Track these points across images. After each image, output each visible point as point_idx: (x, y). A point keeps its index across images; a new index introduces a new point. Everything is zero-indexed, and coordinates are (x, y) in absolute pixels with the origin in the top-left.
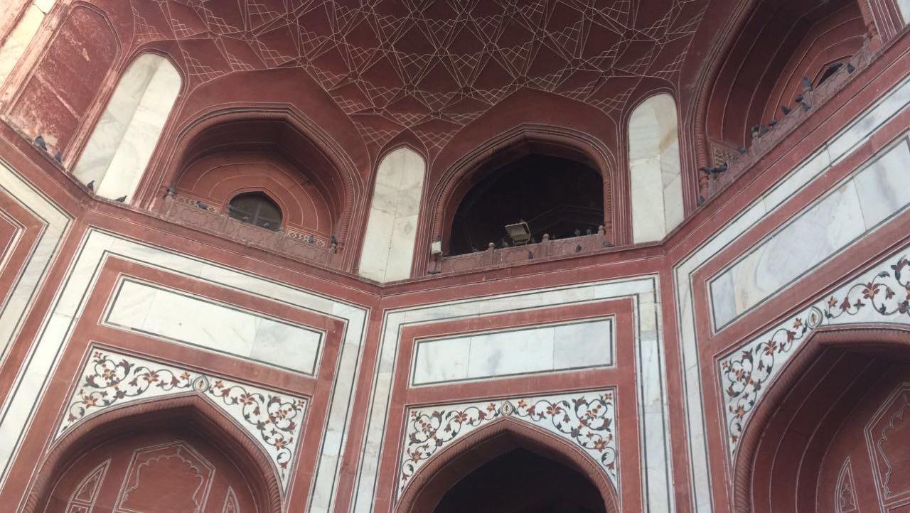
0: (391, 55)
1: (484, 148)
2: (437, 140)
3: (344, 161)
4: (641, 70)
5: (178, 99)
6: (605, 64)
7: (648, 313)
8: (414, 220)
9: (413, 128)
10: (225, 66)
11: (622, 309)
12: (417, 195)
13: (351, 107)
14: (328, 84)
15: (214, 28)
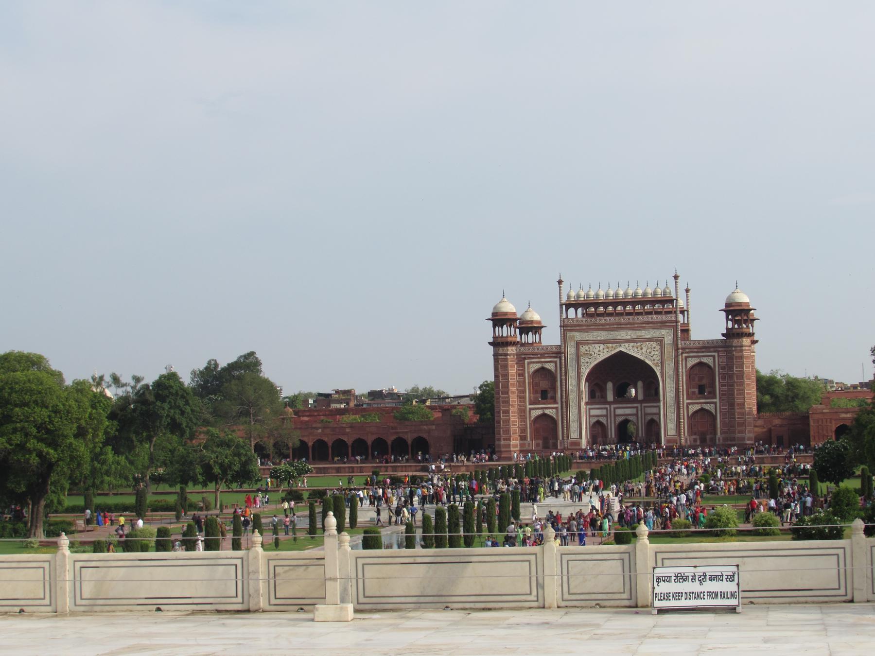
11: (637, 407)
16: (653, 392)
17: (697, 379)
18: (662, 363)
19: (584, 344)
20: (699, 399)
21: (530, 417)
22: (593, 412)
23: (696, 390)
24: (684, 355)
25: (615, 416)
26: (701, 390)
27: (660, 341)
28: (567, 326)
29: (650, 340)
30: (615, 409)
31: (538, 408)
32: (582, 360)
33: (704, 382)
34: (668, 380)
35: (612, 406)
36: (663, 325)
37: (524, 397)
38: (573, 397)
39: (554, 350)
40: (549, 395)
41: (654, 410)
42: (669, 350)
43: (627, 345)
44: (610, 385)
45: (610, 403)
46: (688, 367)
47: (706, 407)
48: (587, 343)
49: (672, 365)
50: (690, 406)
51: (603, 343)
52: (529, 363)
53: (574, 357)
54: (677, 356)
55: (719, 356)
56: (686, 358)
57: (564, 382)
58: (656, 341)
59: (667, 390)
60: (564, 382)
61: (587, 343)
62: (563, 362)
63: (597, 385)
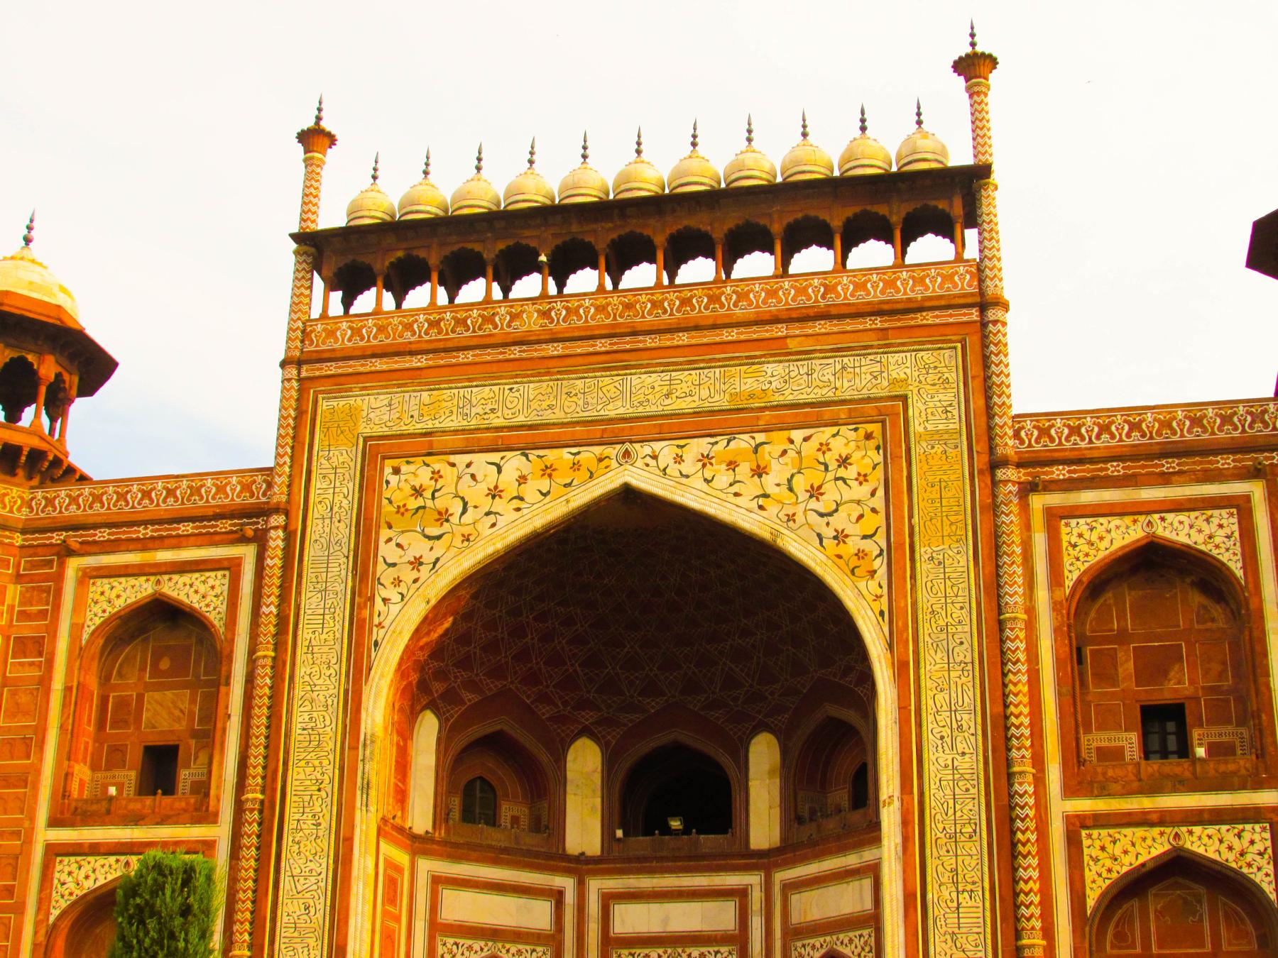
0: (575, 671)
1: (644, 747)
2: (609, 733)
3: (544, 757)
4: (759, 712)
5: (439, 739)
6: (735, 699)
7: (757, 896)
8: (599, 801)
9: (592, 724)
10: (462, 702)
11: (741, 894)
12: (597, 779)
13: (545, 711)
14: (528, 697)
15: (456, 677)
16: (841, 796)
17: (1127, 667)
18: (889, 552)
19: (408, 457)
20: (1153, 789)
21: (44, 902)
22: (462, 906)
23: (1130, 741)
24: (1038, 502)
25: (609, 942)
26: (1164, 726)
27: (885, 417)
28: (320, 358)
29: (812, 414)
30: (608, 900)
31: (95, 849)
32: (387, 551)
33: (1179, 684)
34: (932, 665)
35: (595, 886)
36: (894, 320)
37: (27, 780)
38: (310, 774)
39: (235, 496)
40: (185, 776)
41: (848, 899)
42: (942, 473)
43: (666, 450)
44: (584, 763)
45: (581, 866)
46: (1072, 575)
47: (1204, 843)
48: (425, 446)
49: (960, 560)
50: (1092, 841)
51: (524, 450)
52: (87, 576)
53: (344, 532)
54: (993, 508)
55: (1273, 498)
56: (1054, 517)
57: (264, 681)
58: (854, 420)
59: (930, 731)
60: (264, 681)
61: (425, 446)
62: (274, 562)
63: (496, 744)
